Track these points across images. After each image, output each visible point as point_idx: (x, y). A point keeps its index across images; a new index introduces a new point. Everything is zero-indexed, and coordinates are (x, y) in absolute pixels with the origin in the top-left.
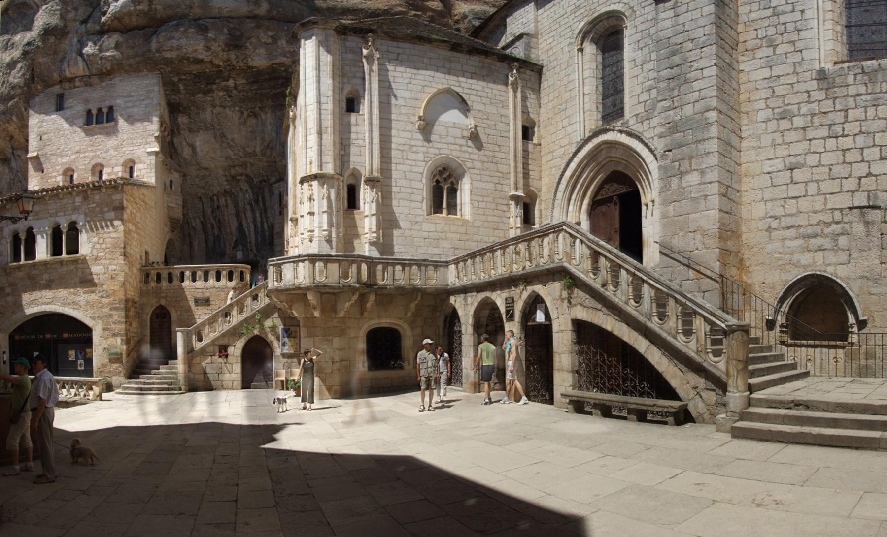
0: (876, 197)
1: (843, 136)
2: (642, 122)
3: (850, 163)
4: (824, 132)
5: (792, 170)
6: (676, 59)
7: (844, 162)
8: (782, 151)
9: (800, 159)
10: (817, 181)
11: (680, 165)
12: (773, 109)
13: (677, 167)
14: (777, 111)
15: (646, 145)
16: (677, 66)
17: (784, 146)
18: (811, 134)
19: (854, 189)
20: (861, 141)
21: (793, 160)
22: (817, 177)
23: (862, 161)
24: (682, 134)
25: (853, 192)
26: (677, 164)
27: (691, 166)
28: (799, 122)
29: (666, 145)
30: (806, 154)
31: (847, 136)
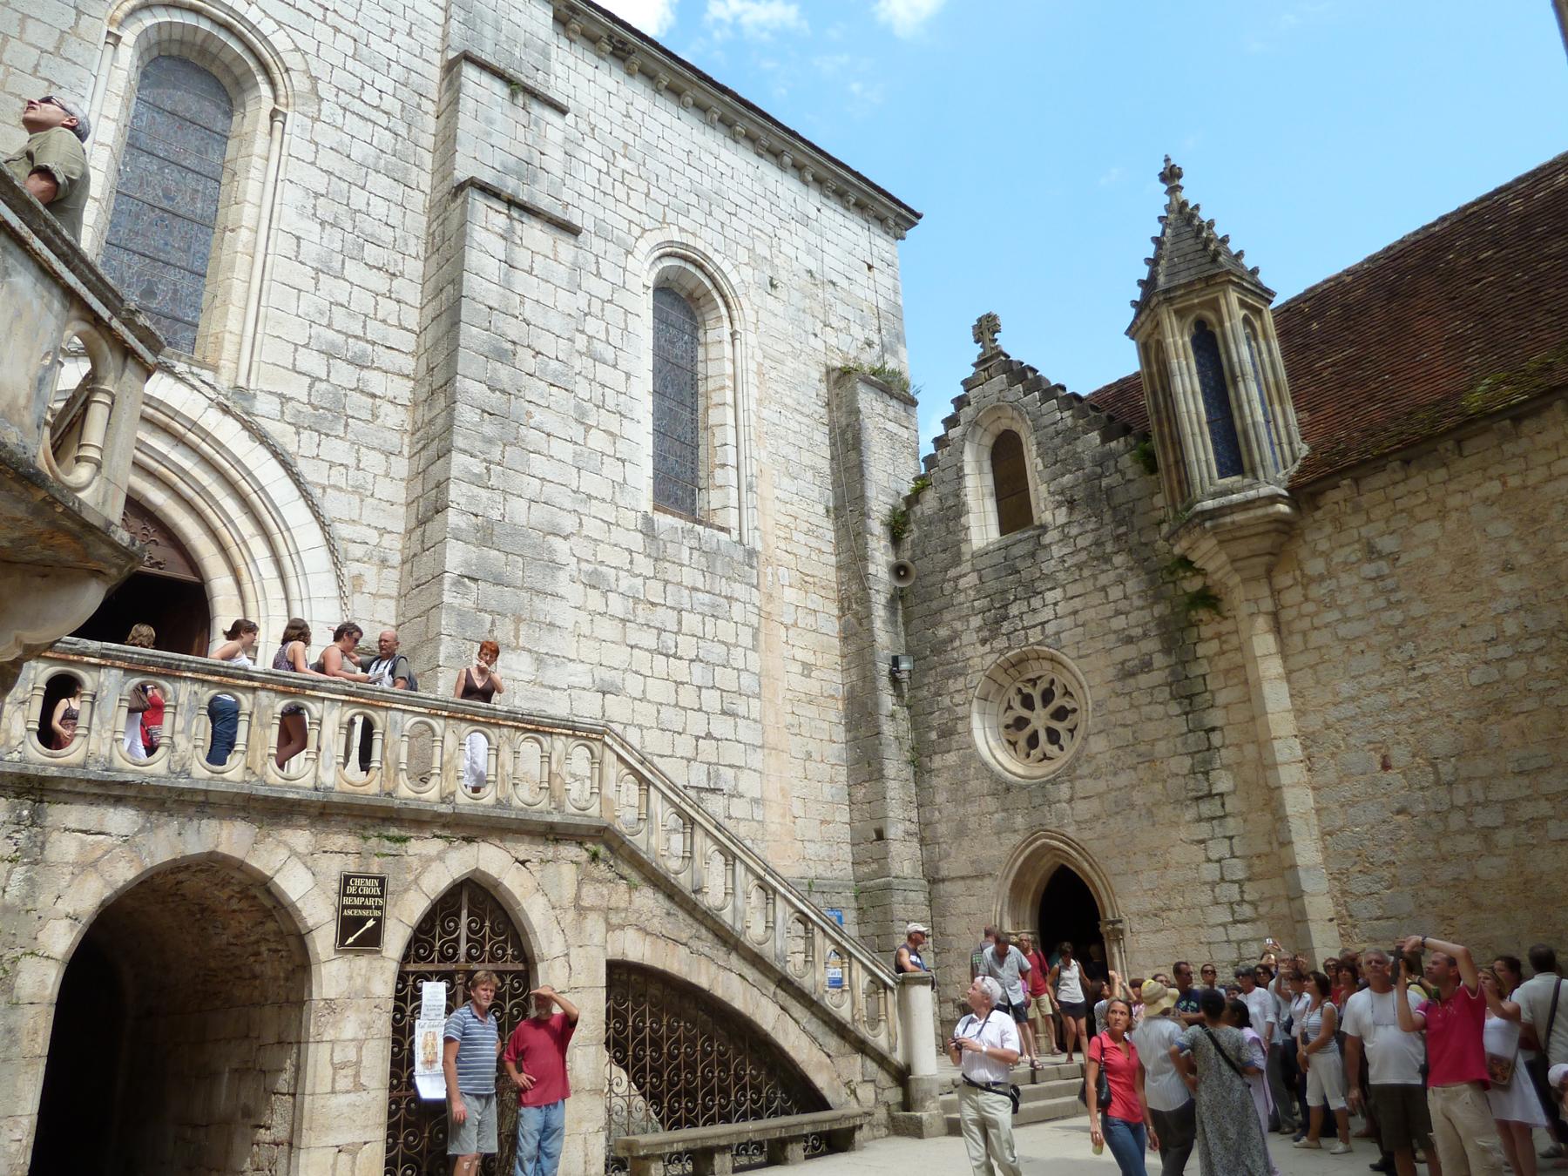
0: (718, 776)
1: (675, 656)
2: (298, 428)
3: (684, 709)
4: (649, 639)
5: (604, 693)
6: (504, 373)
7: (676, 705)
8: (588, 651)
9: (615, 677)
10: (640, 727)
11: (493, 623)
12: (579, 560)
13: (488, 626)
14: (584, 566)
15: (306, 495)
16: (503, 392)
17: (591, 643)
18: (635, 636)
19: (689, 755)
20: (698, 674)
21: (608, 675)
22: (639, 720)
23: (700, 710)
24: (502, 556)
25: (689, 760)
26: (488, 618)
27: (517, 637)
28: (617, 605)
29: (467, 563)
30: (625, 671)
31: (681, 658)
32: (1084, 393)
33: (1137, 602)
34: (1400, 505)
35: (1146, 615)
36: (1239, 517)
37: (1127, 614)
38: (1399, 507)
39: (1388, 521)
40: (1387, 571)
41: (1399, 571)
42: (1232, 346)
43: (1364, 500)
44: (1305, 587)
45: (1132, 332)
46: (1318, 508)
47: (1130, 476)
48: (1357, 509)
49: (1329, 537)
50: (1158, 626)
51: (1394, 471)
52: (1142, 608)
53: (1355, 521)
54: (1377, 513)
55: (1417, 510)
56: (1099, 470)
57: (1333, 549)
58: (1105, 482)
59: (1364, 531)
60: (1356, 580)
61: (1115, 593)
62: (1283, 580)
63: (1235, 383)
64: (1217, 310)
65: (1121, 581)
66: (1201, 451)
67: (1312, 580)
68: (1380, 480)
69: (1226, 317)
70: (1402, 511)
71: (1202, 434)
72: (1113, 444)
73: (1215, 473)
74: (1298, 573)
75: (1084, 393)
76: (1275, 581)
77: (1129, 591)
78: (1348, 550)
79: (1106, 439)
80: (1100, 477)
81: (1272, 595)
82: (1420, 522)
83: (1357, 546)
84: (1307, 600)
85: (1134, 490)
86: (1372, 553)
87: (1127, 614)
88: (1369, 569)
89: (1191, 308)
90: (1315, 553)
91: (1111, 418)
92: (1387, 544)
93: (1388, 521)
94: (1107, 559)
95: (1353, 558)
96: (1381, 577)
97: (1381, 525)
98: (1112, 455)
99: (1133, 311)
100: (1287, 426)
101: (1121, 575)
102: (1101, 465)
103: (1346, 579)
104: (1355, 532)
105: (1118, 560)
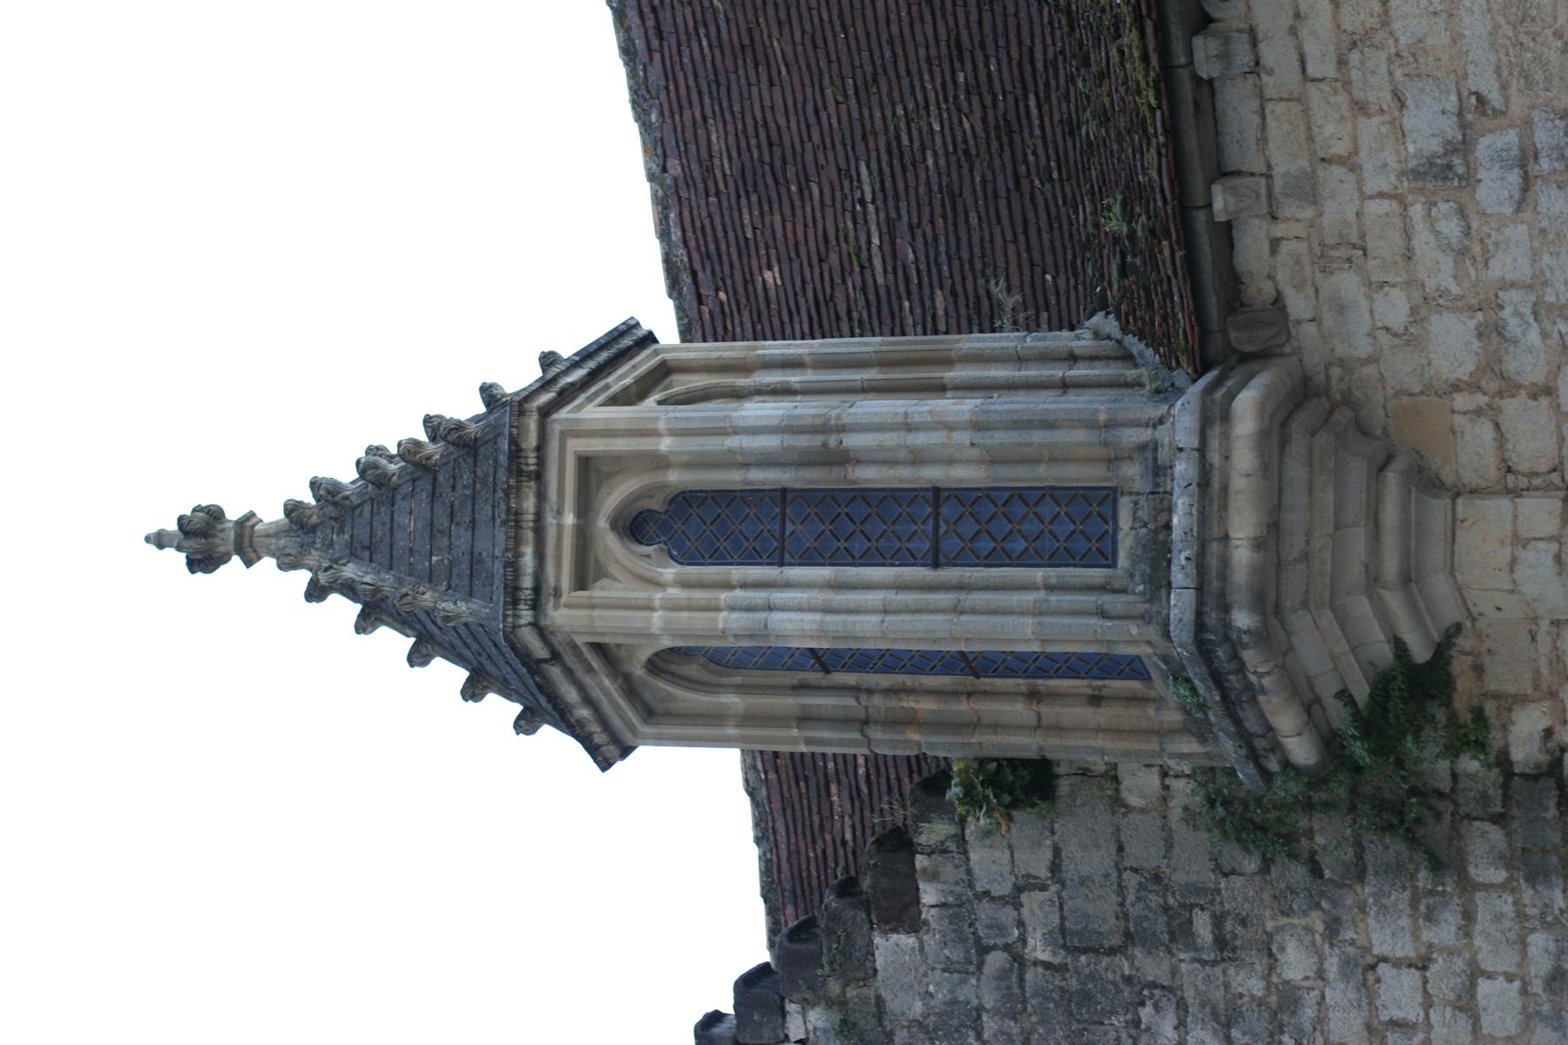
32: (752, 947)
33: (1445, 932)
34: (1320, 66)
35: (1485, 907)
36: (1243, 526)
37: (1475, 973)
38: (1329, 70)
39: (1361, 108)
40: (1512, 137)
41: (1518, 104)
42: (733, 442)
43: (1286, 162)
44: (1510, 388)
45: (607, 749)
46: (1278, 300)
47: (1038, 865)
48: (1308, 190)
49: (1375, 287)
50: (1536, 875)
51: (1225, 56)
52: (1469, 916)
53: (1340, 205)
54: (1333, 133)
55: (1349, 20)
56: (996, 960)
57: (1412, 283)
58: (1038, 949)
59: (1374, 183)
60: (1518, 232)
61: (1399, 994)
62: (1473, 450)
63: (843, 458)
64: (620, 464)
65: (1364, 969)
66: (1017, 609)
67: (1491, 365)
68: (1237, 103)
69: (645, 444)
70: (1342, 62)
71: (962, 587)
72: (929, 895)
73: (1096, 574)
74: (1462, 401)
75: (756, 951)
76: (1469, 477)
77: (1405, 948)
78: (1423, 239)
79: (904, 914)
80: (1019, 961)
81: (1515, 493)
82: (1385, 23)
83: (1417, 211)
84: (1549, 391)
85: (1089, 860)
86: (1445, 171)
87: (1475, 973)
88: (1494, 189)
89: (583, 537)
90: (1411, 338)
91: (847, 888)
92: (1428, 124)
93: (1361, 108)
94: (1289, 998)
95: (1451, 228)
96: (1525, 159)
97: (1369, 128)
98: (957, 911)
99: (547, 732)
100: (1020, 360)
101: (1347, 963)
102: (983, 950)
103: (1510, 263)
104: (1375, 208)
105: (1295, 964)
